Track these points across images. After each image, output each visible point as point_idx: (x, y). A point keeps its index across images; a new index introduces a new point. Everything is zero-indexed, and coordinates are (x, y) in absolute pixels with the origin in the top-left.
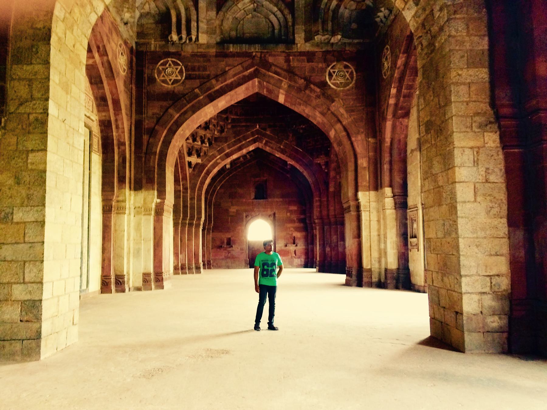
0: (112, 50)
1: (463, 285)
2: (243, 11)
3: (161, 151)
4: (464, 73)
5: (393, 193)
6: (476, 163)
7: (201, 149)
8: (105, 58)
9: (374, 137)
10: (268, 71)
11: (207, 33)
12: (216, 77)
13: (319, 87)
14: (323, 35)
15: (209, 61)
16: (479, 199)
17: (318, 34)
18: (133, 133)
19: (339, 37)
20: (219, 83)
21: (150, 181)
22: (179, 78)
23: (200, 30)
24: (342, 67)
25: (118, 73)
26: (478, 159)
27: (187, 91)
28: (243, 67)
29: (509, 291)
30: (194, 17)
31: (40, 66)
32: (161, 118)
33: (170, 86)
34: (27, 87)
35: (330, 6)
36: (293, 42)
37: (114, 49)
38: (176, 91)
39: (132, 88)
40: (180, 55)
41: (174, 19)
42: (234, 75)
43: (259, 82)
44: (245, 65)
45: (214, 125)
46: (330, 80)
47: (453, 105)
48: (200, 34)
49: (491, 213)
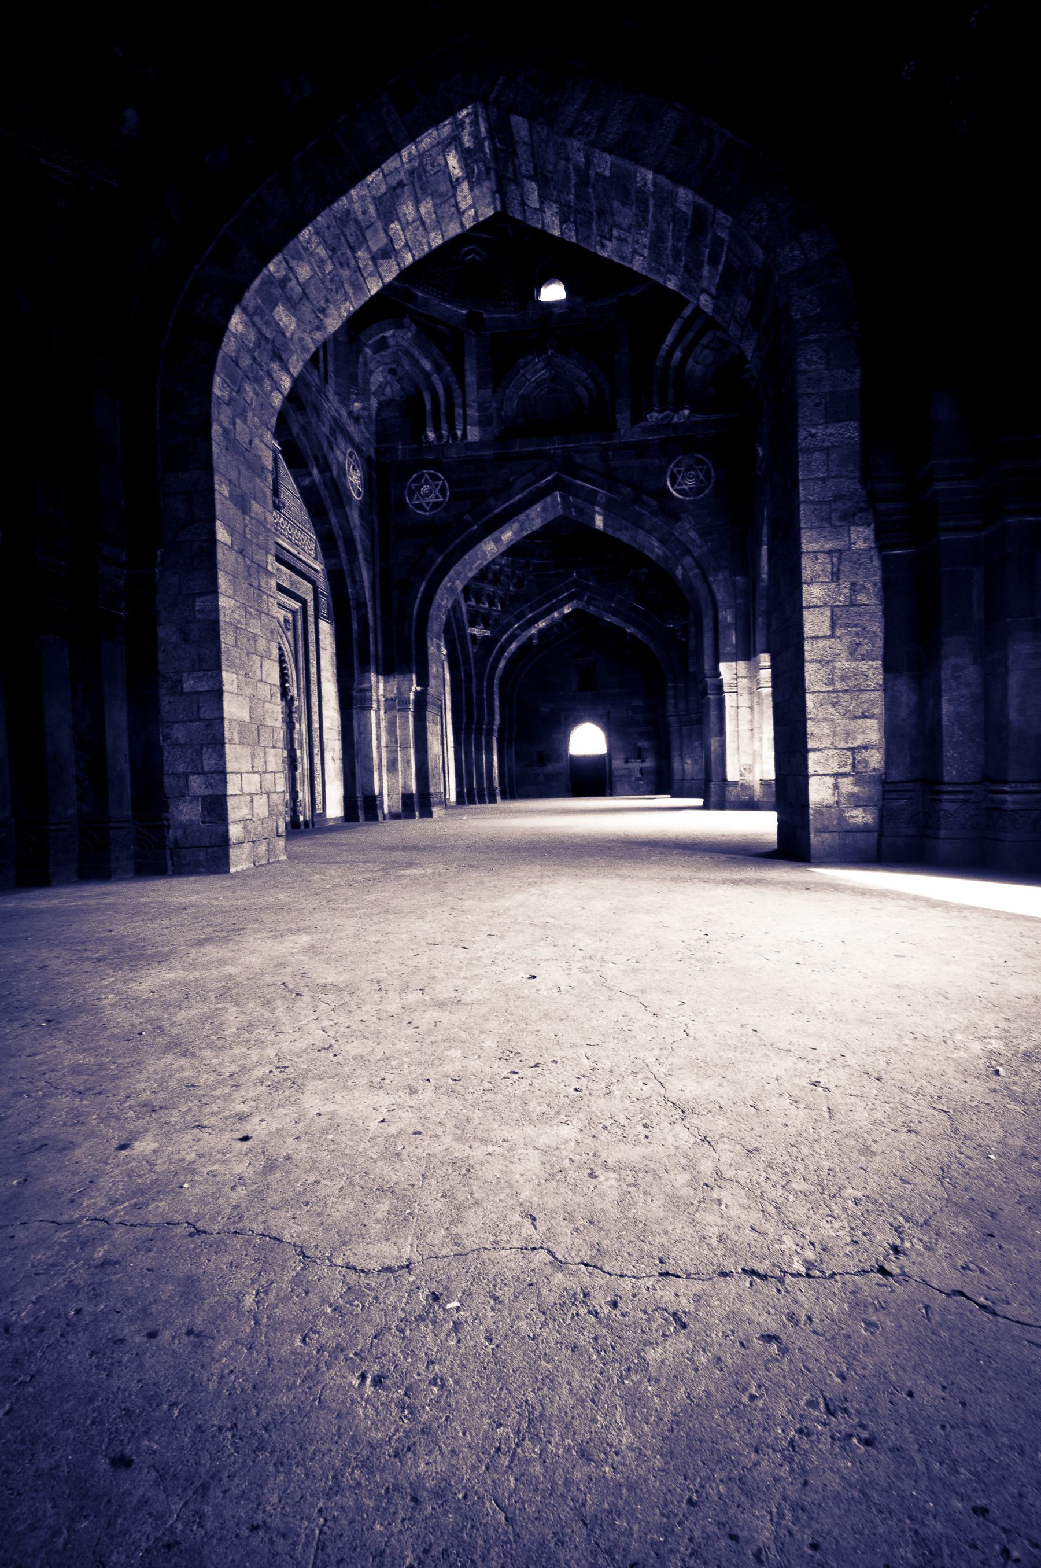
0: (338, 462)
1: (810, 763)
4: (819, 431)
6: (836, 576)
7: (489, 614)
8: (328, 474)
14: (660, 412)
16: (838, 632)
18: (378, 587)
25: (350, 497)
26: (839, 570)
29: (883, 770)
37: (341, 458)
41: (428, 407)
43: (561, 497)
45: (508, 576)
46: (673, 486)
47: (801, 484)
49: (857, 653)
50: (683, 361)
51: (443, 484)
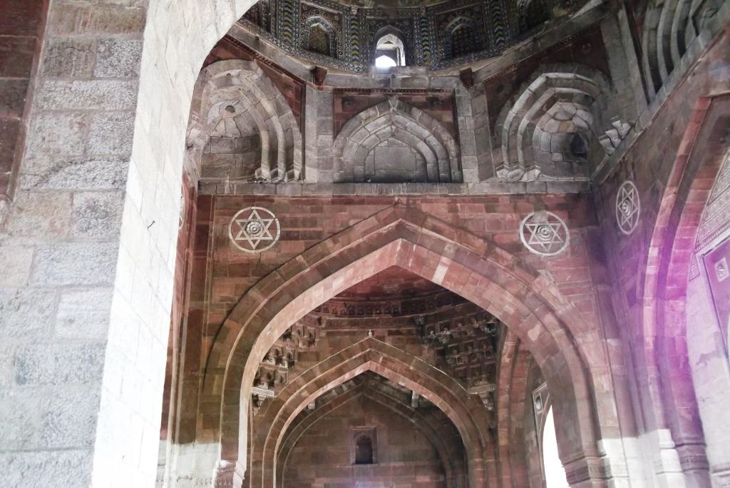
2: (373, 136)
3: (232, 368)
5: (673, 438)
7: (275, 372)
9: (617, 334)
10: (422, 226)
11: (318, 166)
12: (333, 235)
13: (510, 252)
14: (509, 170)
15: (320, 210)
19: (537, 172)
20: (337, 245)
21: (211, 423)
22: (270, 238)
23: (307, 160)
24: (544, 219)
27: (281, 260)
28: (378, 220)
30: (298, 142)
31: (114, 83)
32: (235, 305)
33: (253, 251)
34: (76, 129)
35: (517, 127)
36: (461, 180)
38: (263, 259)
39: (188, 254)
40: (272, 201)
42: (366, 233)
44: (382, 216)
46: (527, 241)
50: (531, 127)
51: (274, 223)
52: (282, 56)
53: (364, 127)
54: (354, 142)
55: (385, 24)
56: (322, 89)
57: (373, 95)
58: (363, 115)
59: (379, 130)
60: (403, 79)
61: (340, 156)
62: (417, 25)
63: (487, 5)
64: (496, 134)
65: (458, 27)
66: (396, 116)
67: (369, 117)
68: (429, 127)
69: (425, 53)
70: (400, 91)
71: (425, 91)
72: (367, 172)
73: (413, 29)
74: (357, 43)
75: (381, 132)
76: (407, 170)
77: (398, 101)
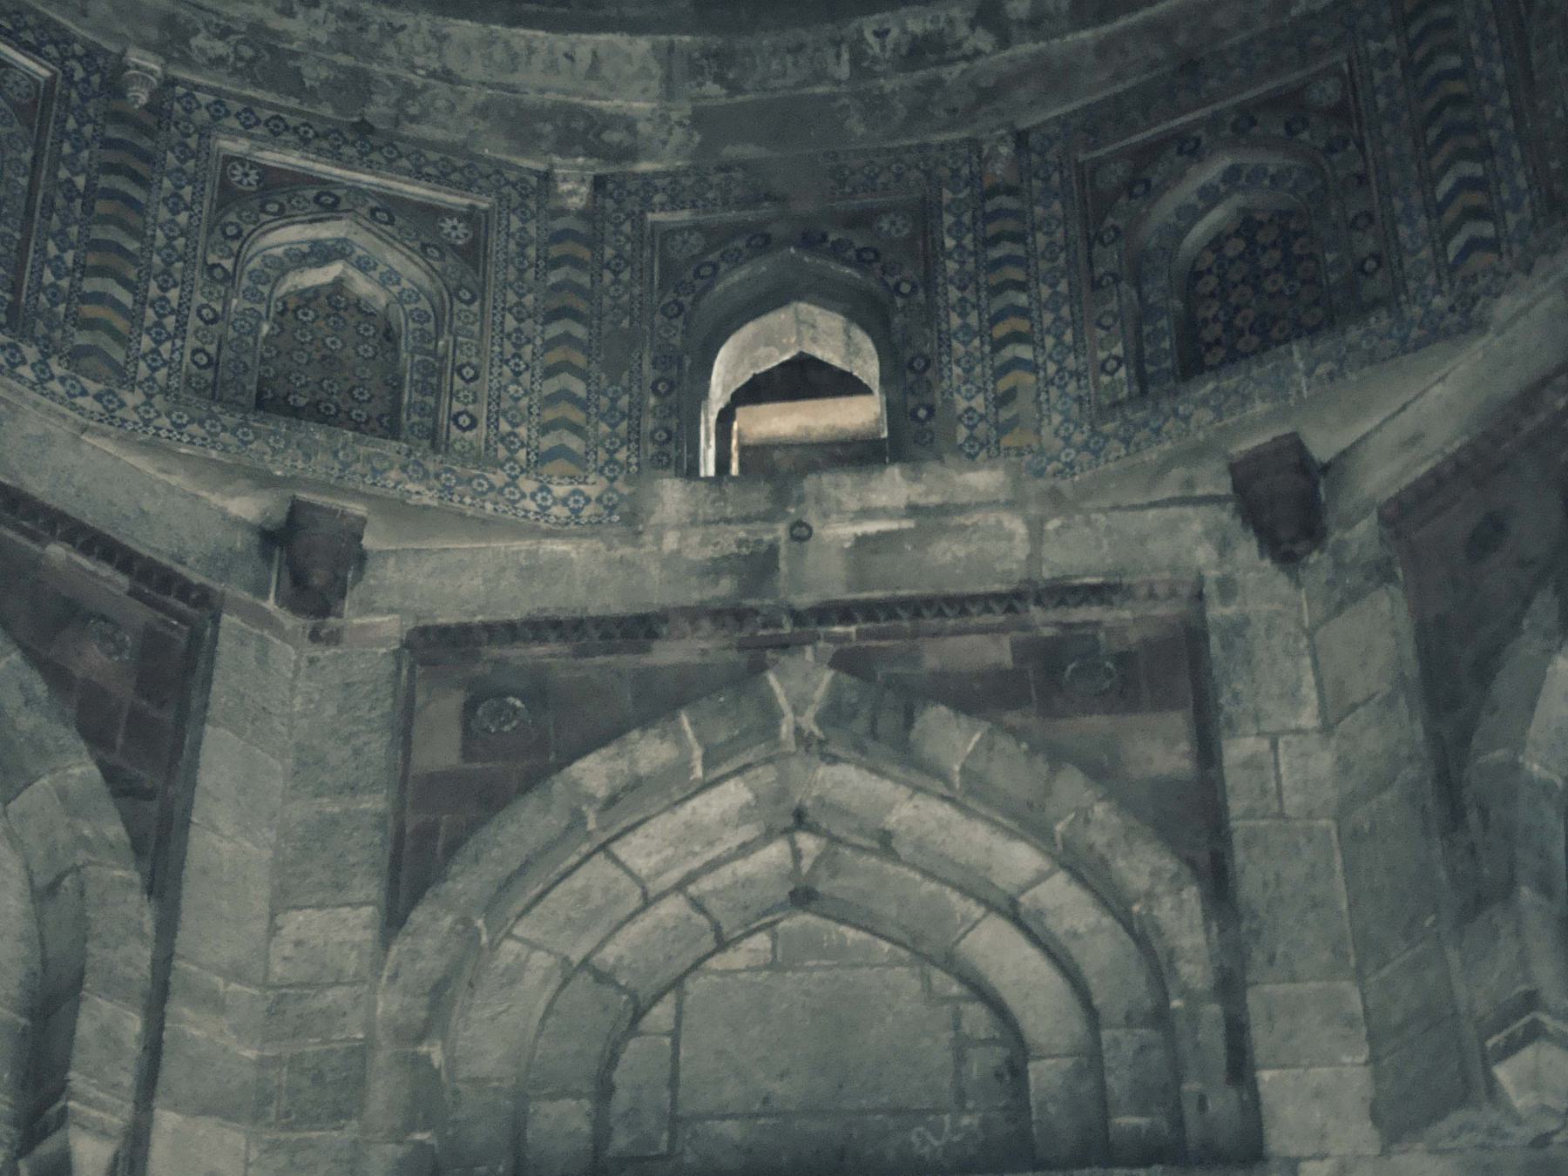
17: (1534, 1033)
23: (172, 1070)
48: (166, 1120)
52: (46, 439)
53: (603, 847)
54: (534, 946)
55: (762, 242)
56: (334, 638)
57: (667, 654)
58: (594, 772)
59: (712, 866)
60: (862, 541)
61: (420, 1038)
62: (958, 229)
63: (1385, 58)
64: (1473, 817)
65: (1217, 216)
66: (823, 771)
67: (636, 784)
68: (1028, 823)
69: (1004, 384)
70: (846, 612)
71: (1011, 601)
72: (621, 1141)
73: (930, 258)
74: (579, 359)
75: (725, 874)
76: (897, 1111)
77: (828, 675)
